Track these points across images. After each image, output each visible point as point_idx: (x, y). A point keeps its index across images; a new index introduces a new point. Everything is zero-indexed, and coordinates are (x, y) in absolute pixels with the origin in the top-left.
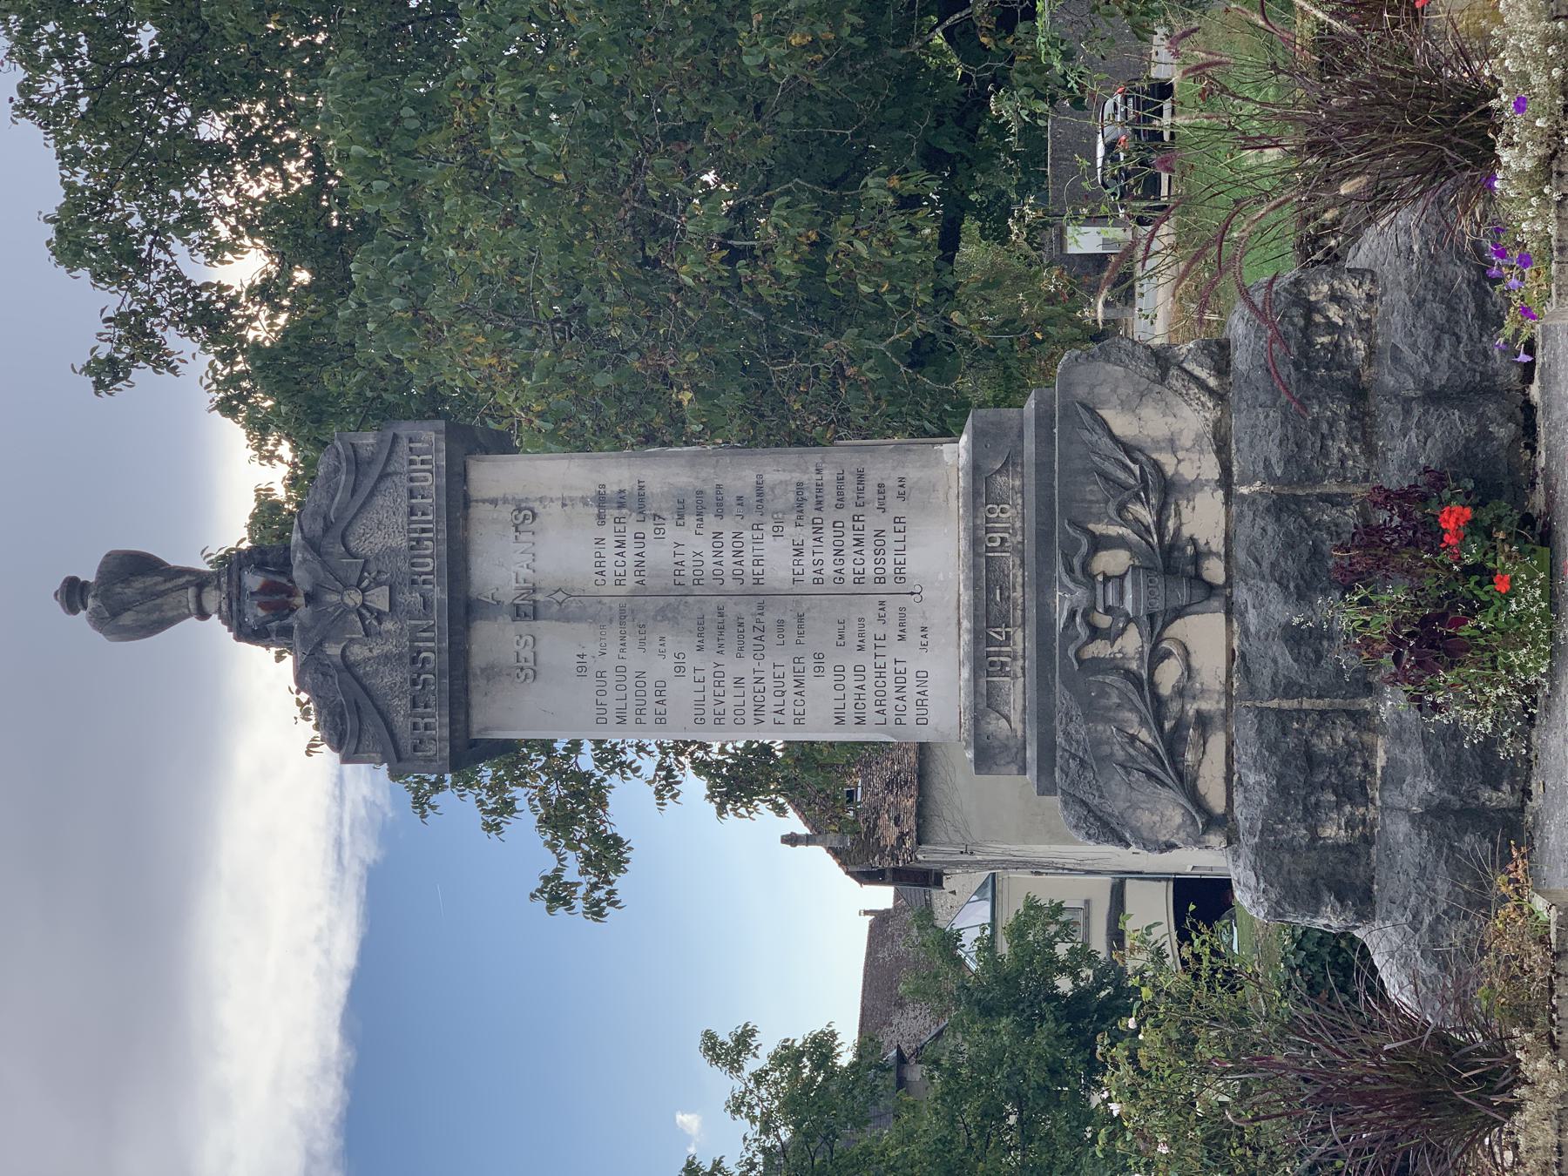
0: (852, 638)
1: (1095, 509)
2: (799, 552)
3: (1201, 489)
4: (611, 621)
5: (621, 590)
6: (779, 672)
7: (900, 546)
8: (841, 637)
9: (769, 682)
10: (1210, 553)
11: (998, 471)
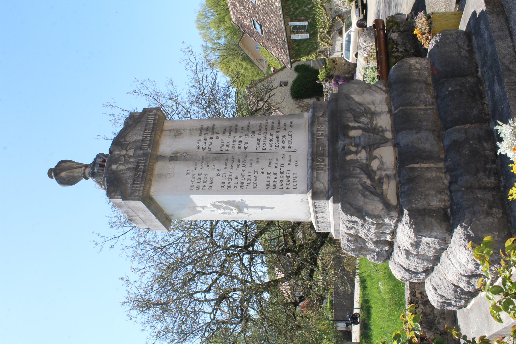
0: (273, 164)
1: (350, 119)
2: (259, 141)
3: (383, 113)
4: (199, 161)
5: (203, 152)
6: (249, 174)
7: (290, 139)
8: (270, 164)
9: (246, 177)
10: (387, 130)
11: (321, 116)
